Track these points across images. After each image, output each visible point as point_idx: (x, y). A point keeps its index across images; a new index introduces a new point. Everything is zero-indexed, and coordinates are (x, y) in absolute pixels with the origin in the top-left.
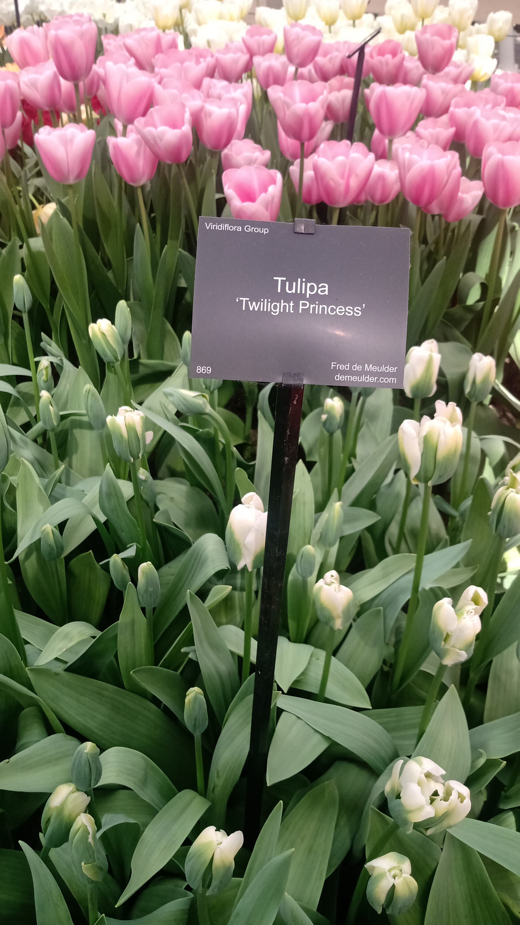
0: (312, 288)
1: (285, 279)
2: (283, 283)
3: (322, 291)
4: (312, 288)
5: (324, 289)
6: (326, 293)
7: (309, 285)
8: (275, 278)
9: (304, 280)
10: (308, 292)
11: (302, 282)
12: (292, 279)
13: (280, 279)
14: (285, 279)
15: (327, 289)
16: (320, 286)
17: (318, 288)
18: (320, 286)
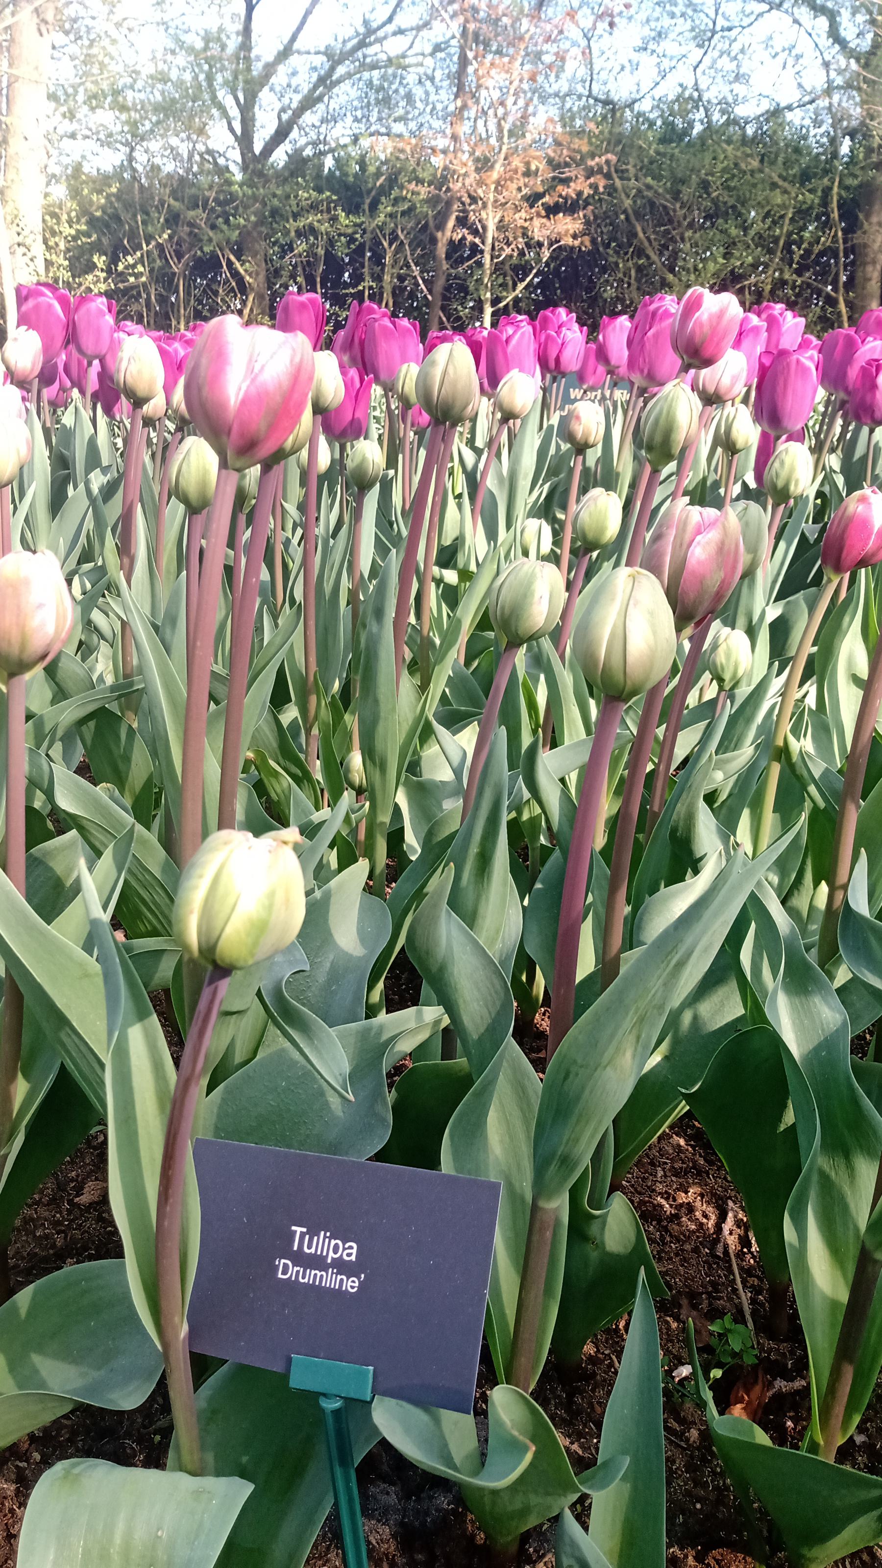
0: (336, 1250)
1: (304, 1230)
2: (303, 1235)
3: (349, 1255)
4: (336, 1250)
5: (350, 1252)
6: (353, 1258)
7: (333, 1242)
8: (294, 1228)
9: (328, 1234)
10: (331, 1254)
11: (325, 1237)
12: (313, 1232)
13: (299, 1230)
14: (304, 1230)
15: (354, 1251)
16: (347, 1246)
17: (344, 1249)
18: (347, 1246)
